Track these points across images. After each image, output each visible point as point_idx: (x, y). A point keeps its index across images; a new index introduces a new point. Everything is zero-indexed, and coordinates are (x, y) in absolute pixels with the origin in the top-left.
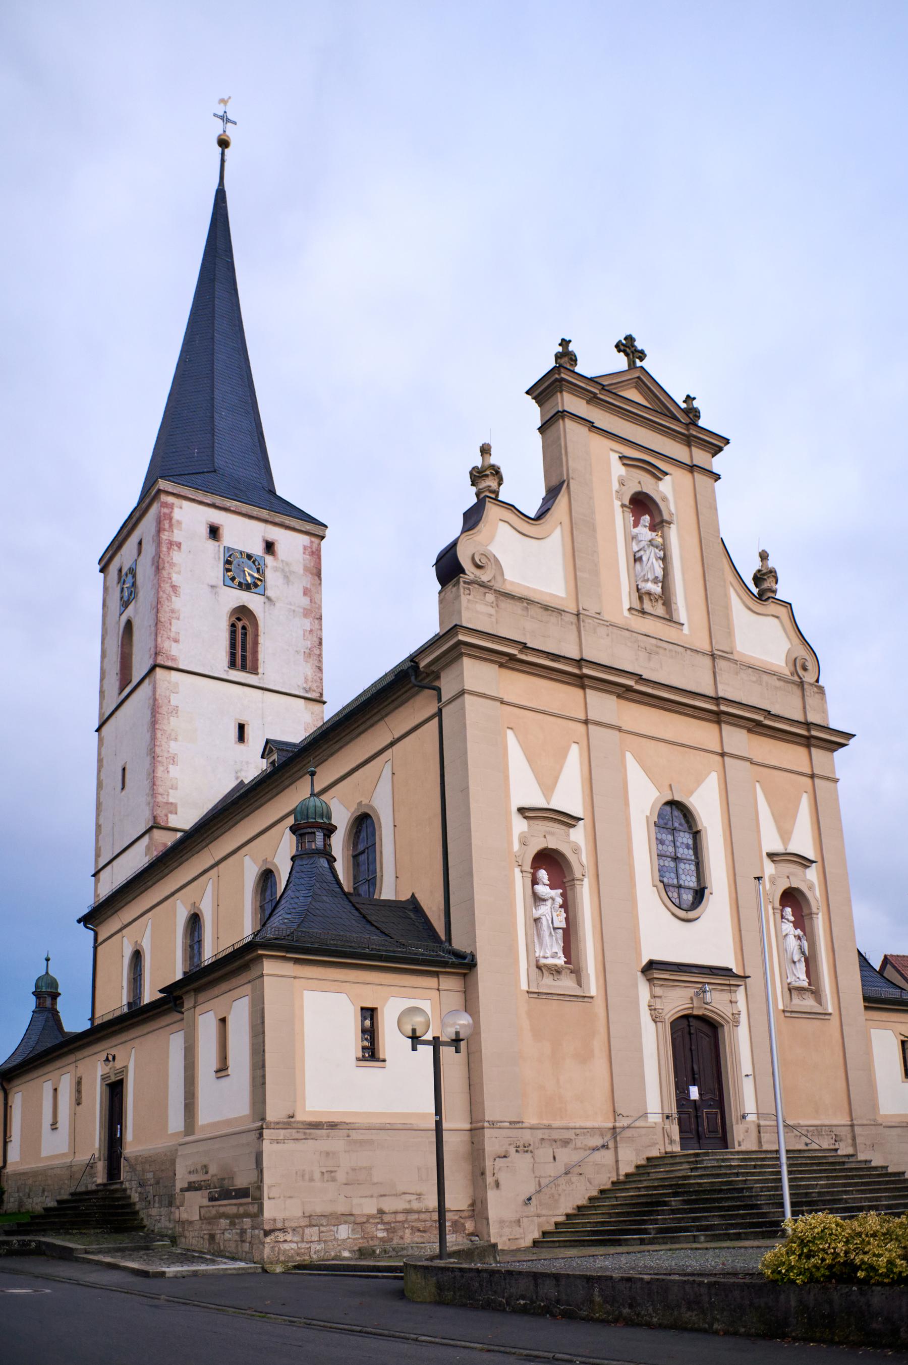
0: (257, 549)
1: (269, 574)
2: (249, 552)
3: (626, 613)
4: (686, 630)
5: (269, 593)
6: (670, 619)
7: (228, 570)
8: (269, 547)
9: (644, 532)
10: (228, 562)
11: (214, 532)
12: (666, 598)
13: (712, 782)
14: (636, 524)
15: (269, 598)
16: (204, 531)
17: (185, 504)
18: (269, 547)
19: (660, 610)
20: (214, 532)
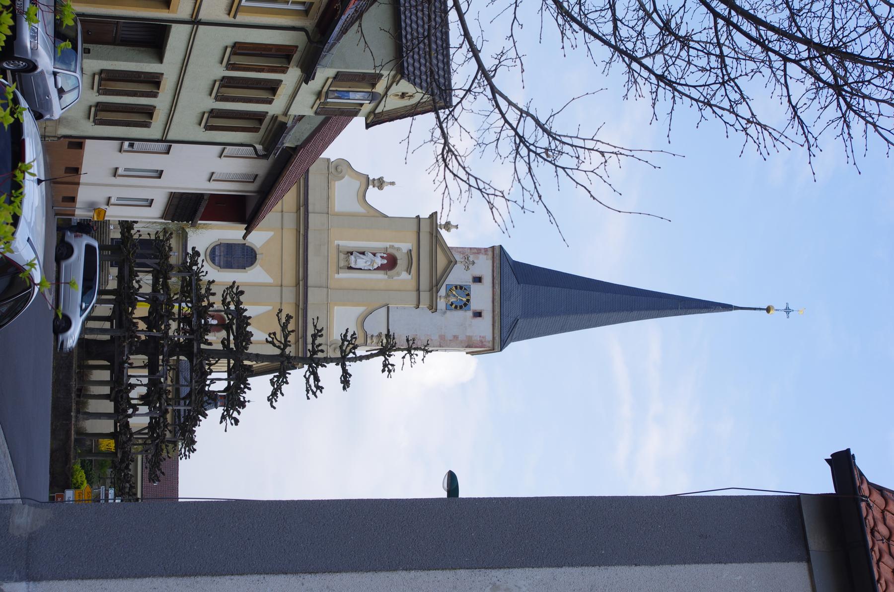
0: (475, 305)
1: (460, 313)
2: (471, 301)
3: (336, 242)
4: (336, 276)
5: (448, 312)
6: (339, 269)
7: (456, 287)
8: (478, 314)
9: (379, 262)
10: (461, 288)
11: (478, 280)
12: (350, 268)
13: (268, 279)
14: (382, 257)
15: (445, 313)
16: (477, 274)
17: (490, 262)
18: (478, 314)
19: (342, 264)
20: (478, 280)
